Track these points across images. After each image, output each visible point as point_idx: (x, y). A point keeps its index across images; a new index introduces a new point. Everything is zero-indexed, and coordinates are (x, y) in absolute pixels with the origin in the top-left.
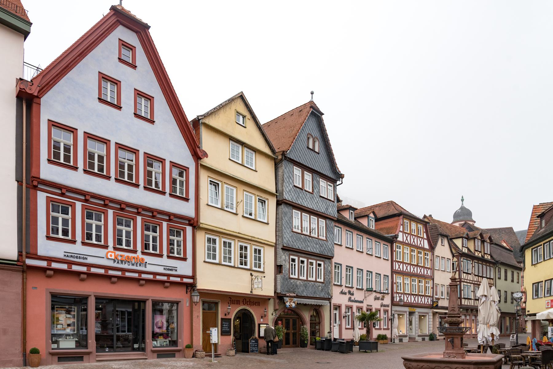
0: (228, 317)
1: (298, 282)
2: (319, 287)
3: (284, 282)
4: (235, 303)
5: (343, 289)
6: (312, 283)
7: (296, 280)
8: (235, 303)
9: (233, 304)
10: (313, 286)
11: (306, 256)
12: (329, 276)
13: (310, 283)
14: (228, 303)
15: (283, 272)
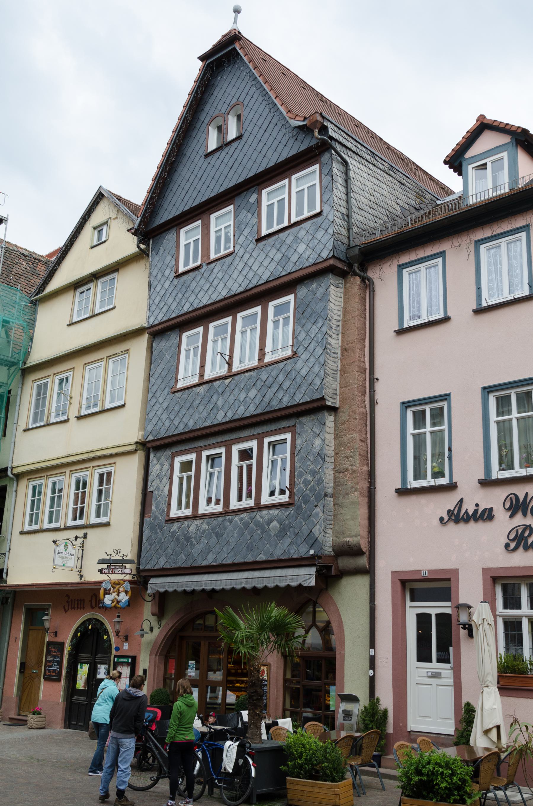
0: (59, 639)
1: (193, 526)
2: (269, 524)
3: (151, 536)
4: (76, 606)
5: (461, 500)
6: (244, 515)
7: (186, 523)
8: (76, 606)
9: (72, 609)
10: (246, 525)
11: (220, 439)
12: (314, 473)
13: (236, 519)
14: (64, 607)
15: (153, 508)
